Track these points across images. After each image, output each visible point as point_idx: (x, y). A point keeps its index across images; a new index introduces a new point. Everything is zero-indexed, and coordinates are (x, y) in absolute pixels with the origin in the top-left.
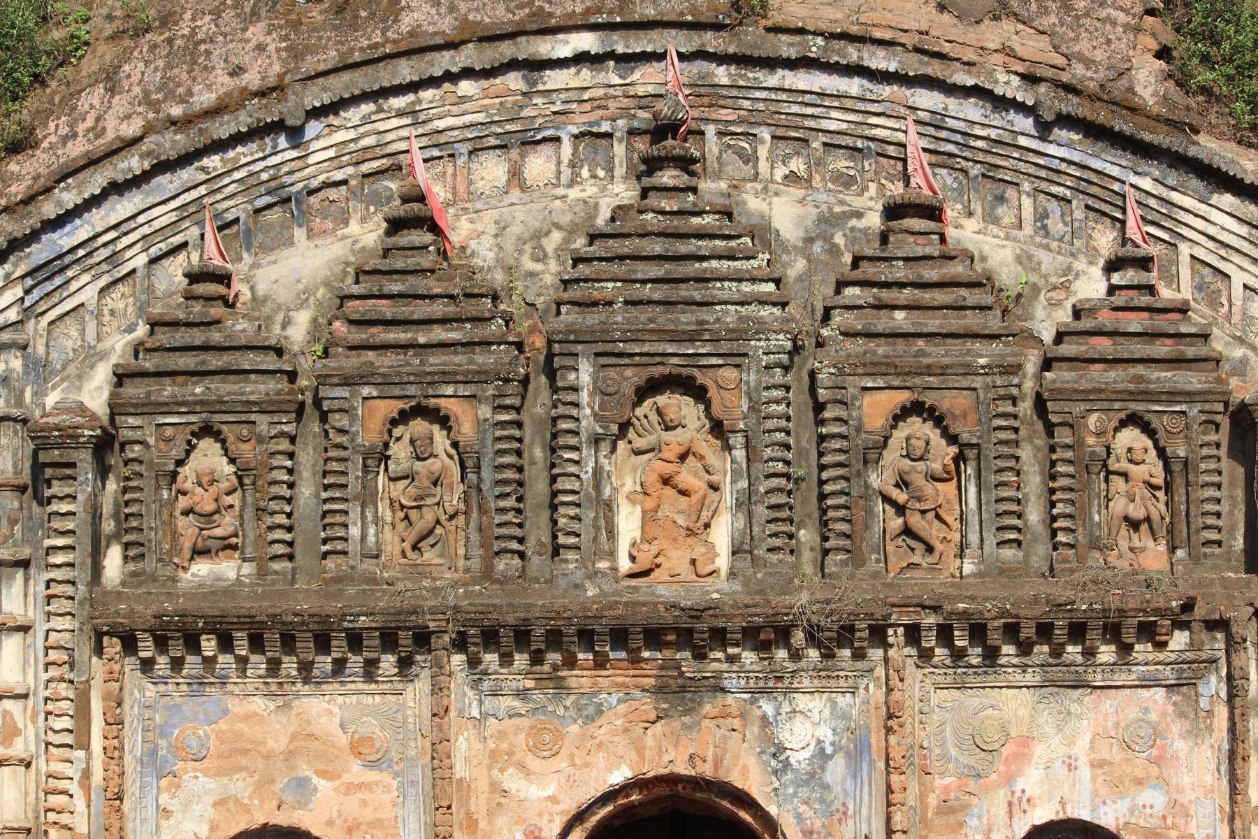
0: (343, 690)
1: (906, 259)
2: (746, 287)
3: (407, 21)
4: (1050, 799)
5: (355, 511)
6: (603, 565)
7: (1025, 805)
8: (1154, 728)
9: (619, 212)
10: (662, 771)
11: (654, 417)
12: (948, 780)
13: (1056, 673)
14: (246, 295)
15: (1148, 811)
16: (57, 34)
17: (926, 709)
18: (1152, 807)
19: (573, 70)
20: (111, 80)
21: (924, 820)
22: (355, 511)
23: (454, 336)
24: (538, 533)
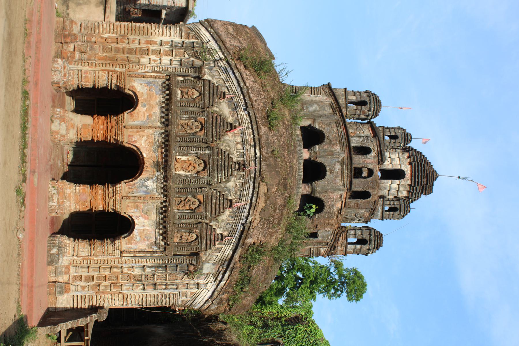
3: (262, 127)
5: (187, 116)
6: (178, 154)
9: (232, 159)
11: (200, 163)
13: (158, 224)
14: (221, 101)
16: (262, 74)
20: (255, 82)
21: (136, 202)
22: (187, 116)
24: (183, 144)
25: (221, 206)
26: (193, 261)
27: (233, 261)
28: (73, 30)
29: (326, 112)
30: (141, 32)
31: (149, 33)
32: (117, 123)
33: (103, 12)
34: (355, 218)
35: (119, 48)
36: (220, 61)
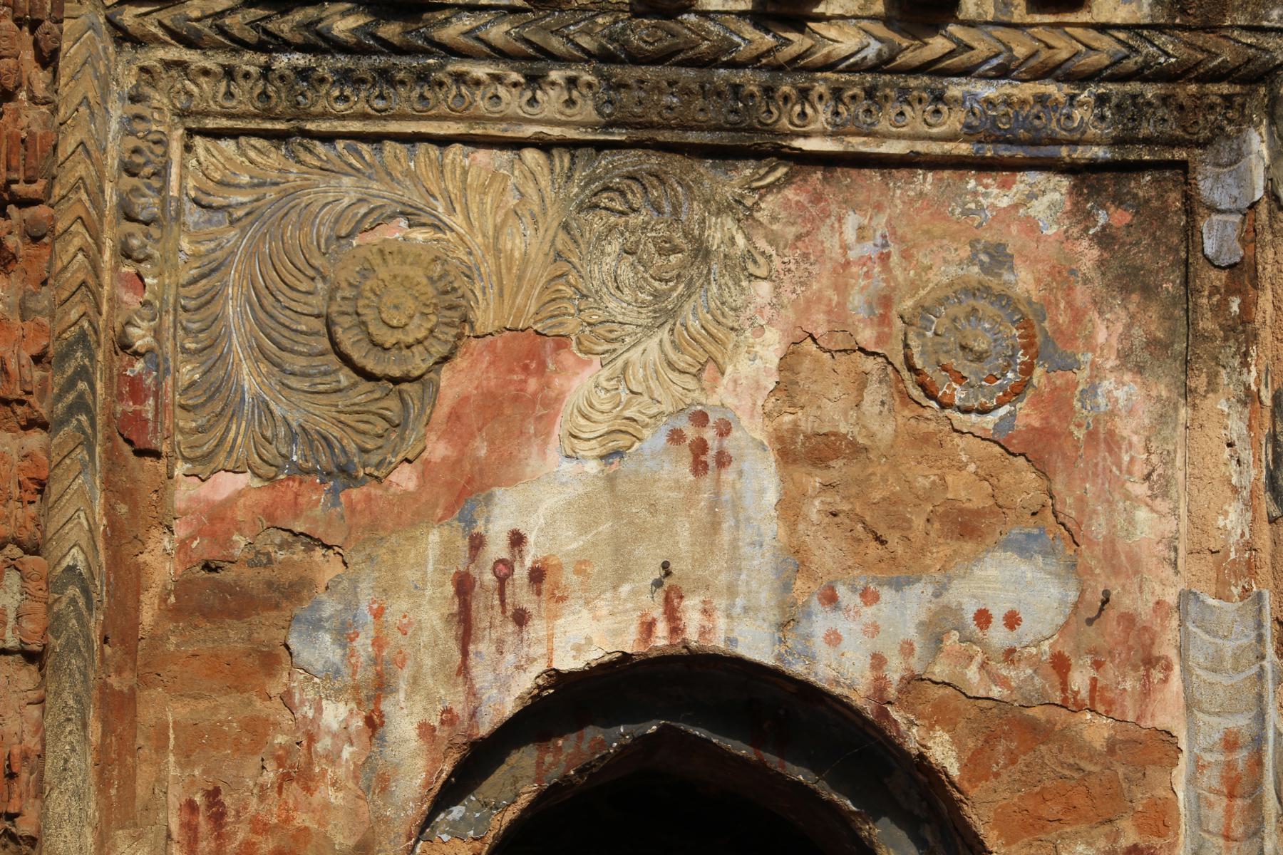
4: (621, 576)
7: (521, 594)
8: (1025, 324)
12: (227, 485)
15: (998, 635)
17: (148, 204)
18: (1012, 621)
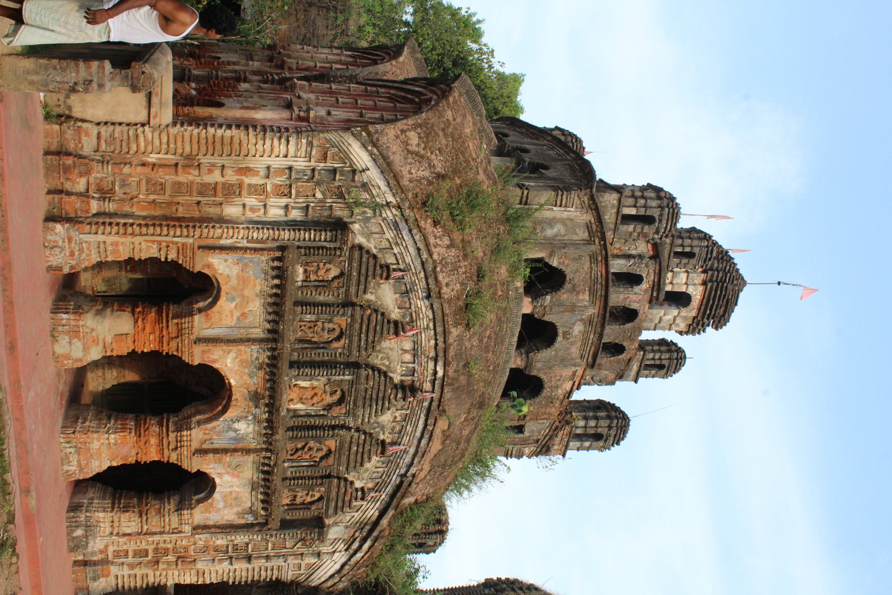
0: (261, 311)
1: (370, 450)
2: (367, 416)
9: (391, 378)
10: (233, 393)
13: (256, 485)
19: (433, 368)
23: (362, 343)
25: (365, 456)
26: (313, 535)
27: (379, 528)
28: (83, 146)
29: (575, 237)
30: (227, 149)
31: (243, 149)
32: (180, 333)
33: (144, 102)
34: (592, 382)
35: (180, 183)
36: (386, 208)
